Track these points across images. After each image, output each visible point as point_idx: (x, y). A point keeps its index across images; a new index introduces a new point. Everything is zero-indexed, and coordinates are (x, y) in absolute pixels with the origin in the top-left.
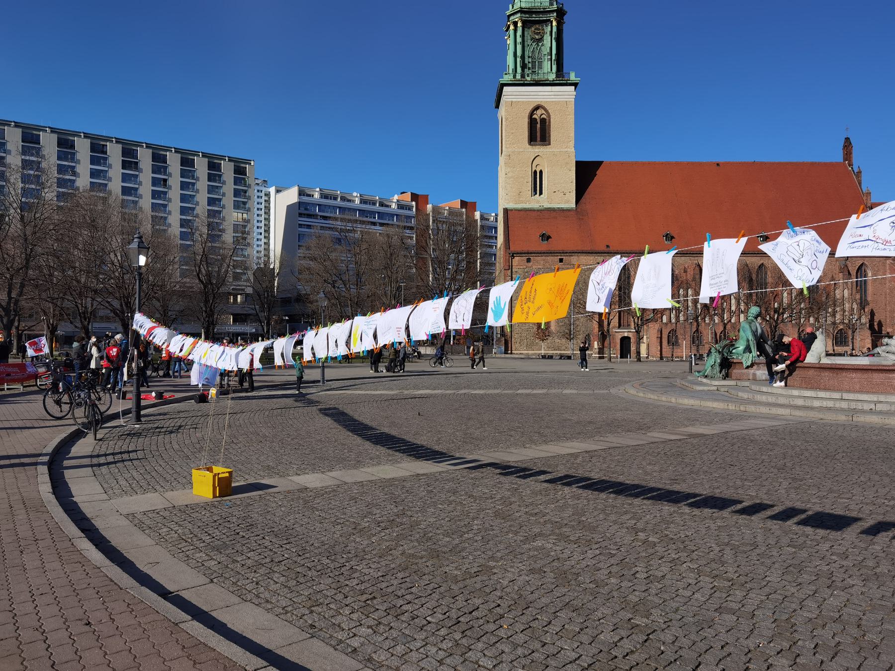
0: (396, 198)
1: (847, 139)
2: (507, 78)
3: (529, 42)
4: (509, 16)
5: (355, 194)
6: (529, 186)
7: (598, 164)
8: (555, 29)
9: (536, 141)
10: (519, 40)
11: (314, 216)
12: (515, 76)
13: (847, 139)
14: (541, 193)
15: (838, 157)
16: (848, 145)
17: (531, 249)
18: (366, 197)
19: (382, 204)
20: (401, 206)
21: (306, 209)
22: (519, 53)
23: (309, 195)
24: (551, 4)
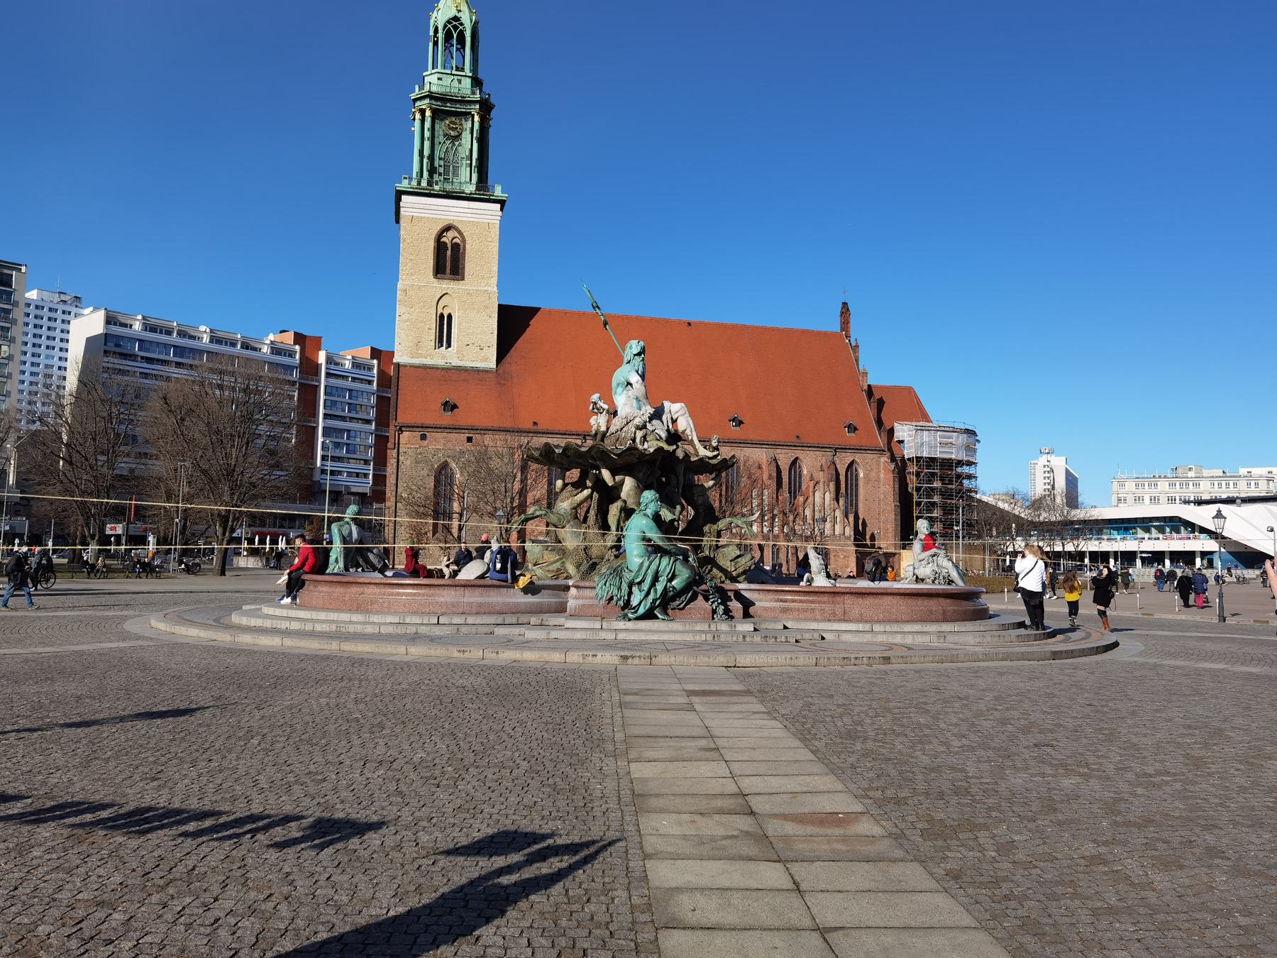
1: (845, 304)
3: (442, 139)
4: (415, 100)
5: (203, 328)
6: (432, 335)
11: (132, 357)
13: (845, 304)
14: (449, 345)
17: (427, 422)
18: (220, 334)
19: (246, 346)
21: (118, 345)
23: (125, 325)
24: (473, 93)
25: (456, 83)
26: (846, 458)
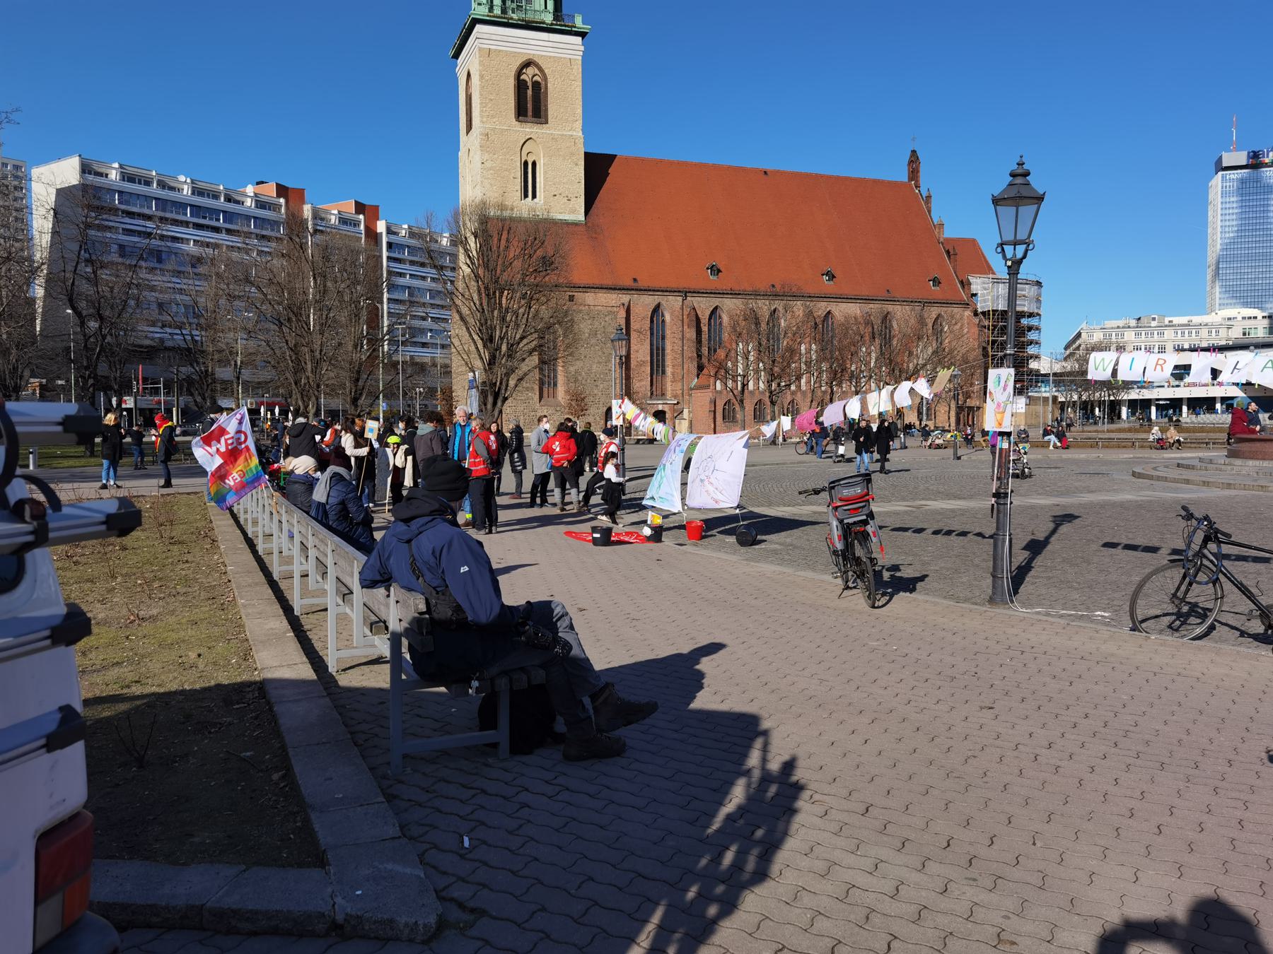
0: (250, 190)
1: (914, 152)
2: (481, 11)
5: (182, 178)
7: (610, 159)
9: (526, 115)
12: (491, 9)
13: (914, 152)
14: (534, 196)
15: (903, 176)
16: (914, 159)
20: (261, 204)
23: (101, 174)
26: (934, 312)
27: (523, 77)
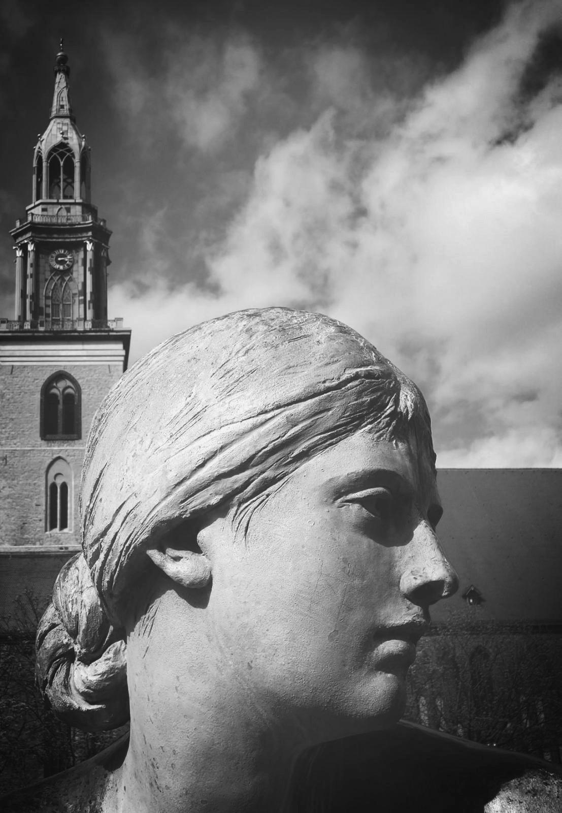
3: (48, 275)
8: (90, 256)
10: (30, 271)
14: (64, 525)
22: (29, 291)
24: (84, 219)
25: (64, 212)
27: (54, 391)
